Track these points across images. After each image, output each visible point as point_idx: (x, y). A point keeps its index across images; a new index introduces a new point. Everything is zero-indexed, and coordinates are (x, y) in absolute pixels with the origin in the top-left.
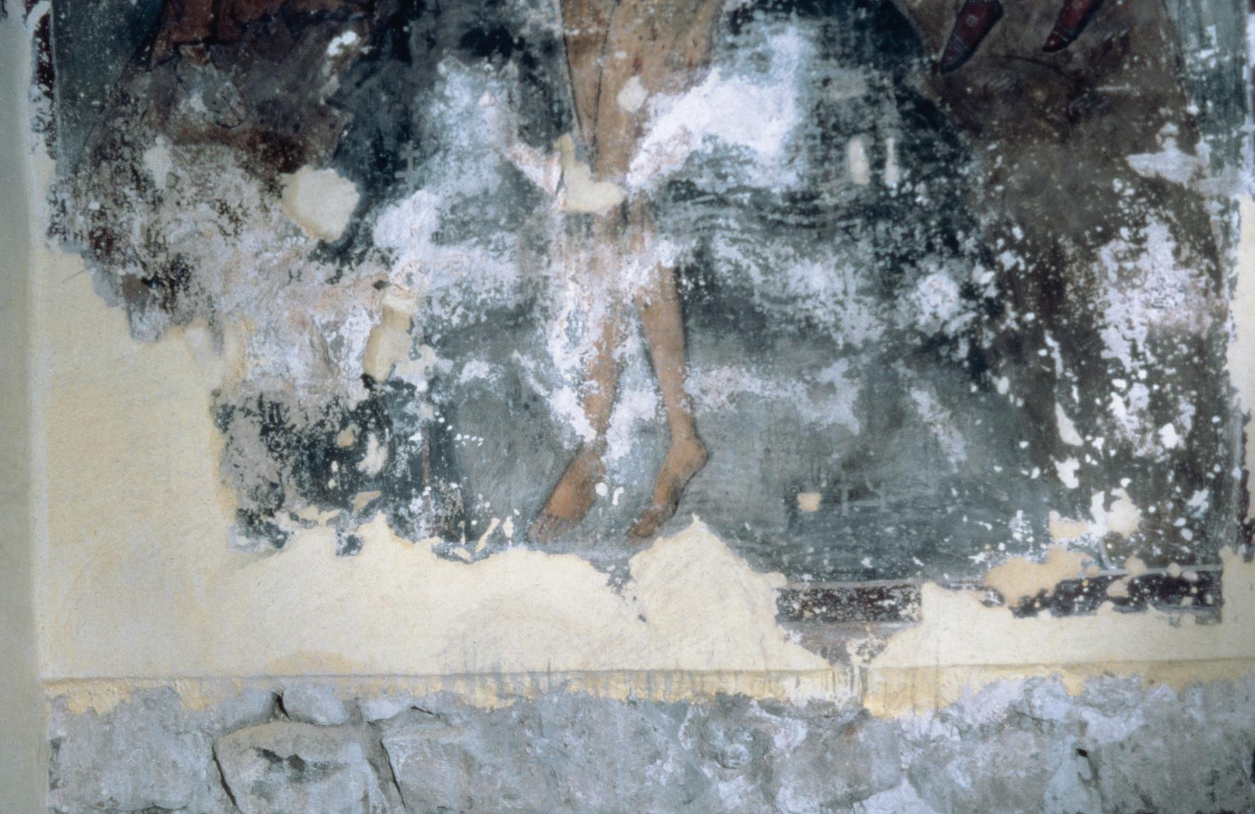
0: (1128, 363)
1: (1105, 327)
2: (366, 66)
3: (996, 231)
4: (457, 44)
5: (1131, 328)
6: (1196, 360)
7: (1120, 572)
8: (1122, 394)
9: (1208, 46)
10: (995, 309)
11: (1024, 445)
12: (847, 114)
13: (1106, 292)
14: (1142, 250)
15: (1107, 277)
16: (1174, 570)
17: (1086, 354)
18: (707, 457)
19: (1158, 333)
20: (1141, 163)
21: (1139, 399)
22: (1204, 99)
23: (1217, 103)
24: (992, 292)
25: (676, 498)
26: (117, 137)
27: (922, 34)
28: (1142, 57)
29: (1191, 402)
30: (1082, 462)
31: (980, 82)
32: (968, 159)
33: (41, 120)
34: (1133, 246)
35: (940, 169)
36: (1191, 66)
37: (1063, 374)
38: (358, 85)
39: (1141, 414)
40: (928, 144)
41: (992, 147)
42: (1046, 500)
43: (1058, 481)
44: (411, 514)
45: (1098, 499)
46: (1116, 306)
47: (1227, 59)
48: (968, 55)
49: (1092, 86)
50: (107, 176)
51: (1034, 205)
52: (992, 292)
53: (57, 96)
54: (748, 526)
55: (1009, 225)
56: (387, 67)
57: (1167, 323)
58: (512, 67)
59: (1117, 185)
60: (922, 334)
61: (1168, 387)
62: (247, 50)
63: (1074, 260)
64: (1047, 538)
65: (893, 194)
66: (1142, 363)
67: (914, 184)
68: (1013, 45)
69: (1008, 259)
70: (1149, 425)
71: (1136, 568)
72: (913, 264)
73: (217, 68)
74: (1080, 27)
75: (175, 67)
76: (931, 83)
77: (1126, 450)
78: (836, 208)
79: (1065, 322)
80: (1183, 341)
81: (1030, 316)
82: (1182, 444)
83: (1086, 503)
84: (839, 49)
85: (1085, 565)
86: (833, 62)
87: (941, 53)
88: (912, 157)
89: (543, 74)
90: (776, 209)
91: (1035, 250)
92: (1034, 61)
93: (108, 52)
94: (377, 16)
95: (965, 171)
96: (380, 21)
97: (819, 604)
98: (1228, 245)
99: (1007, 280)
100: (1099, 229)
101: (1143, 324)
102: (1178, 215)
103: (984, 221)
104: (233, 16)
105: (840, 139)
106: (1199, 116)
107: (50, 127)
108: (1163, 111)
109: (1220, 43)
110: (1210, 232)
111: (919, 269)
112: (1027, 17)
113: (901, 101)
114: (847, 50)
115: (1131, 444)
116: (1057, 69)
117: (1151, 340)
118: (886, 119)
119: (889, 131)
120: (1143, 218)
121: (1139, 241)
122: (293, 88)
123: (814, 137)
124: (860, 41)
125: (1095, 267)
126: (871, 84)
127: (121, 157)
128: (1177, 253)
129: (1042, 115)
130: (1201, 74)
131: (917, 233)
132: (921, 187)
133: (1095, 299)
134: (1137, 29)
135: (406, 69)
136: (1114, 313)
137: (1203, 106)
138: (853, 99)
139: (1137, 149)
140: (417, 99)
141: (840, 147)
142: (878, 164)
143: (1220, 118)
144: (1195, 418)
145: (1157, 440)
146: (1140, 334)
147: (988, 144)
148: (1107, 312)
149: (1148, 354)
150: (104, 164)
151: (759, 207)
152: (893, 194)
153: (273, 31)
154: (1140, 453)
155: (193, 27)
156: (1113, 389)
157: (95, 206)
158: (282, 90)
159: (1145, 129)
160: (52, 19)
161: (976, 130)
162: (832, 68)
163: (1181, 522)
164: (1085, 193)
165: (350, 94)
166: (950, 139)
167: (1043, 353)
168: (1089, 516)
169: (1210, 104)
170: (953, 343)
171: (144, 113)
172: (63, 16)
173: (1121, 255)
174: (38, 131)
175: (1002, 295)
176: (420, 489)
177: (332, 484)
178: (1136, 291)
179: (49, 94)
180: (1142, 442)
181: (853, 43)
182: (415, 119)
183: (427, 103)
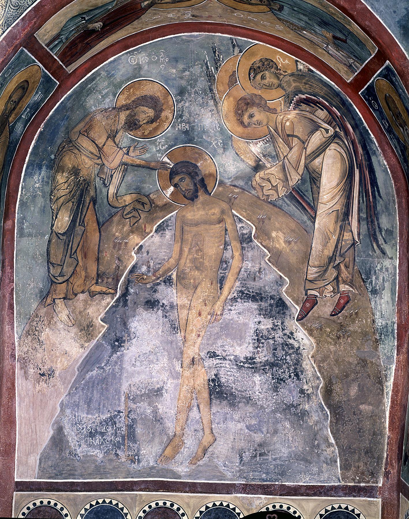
12: (265, 333)
72: (284, 381)
78: (261, 362)
84: (264, 312)
86: (262, 316)
105: (263, 341)
123: (255, 340)
124: (271, 310)
127: (35, 334)
129: (329, 336)
162: (261, 318)
181: (269, 310)
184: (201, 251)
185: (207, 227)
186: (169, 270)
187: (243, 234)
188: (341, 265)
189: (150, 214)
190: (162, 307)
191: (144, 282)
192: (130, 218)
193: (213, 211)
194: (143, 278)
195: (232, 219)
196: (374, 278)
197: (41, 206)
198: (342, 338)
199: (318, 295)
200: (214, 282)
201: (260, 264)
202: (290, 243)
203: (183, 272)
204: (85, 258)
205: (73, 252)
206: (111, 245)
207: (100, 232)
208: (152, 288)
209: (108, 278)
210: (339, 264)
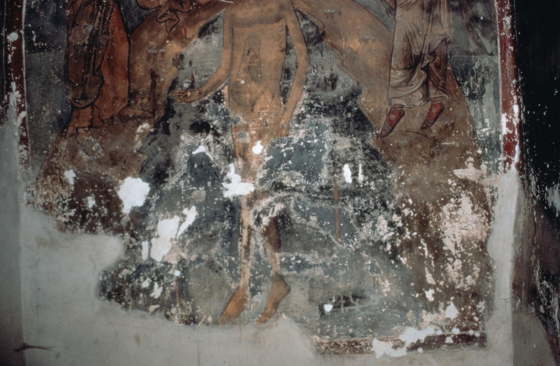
0: (454, 251)
1: (444, 237)
2: (152, 137)
3: (402, 201)
4: (189, 128)
5: (455, 238)
6: (480, 250)
7: (450, 333)
8: (451, 264)
9: (486, 127)
10: (401, 231)
11: (412, 284)
12: (343, 155)
13: (445, 224)
14: (459, 207)
15: (445, 218)
16: (471, 332)
17: (437, 249)
18: (289, 290)
19: (465, 239)
20: (459, 173)
21: (458, 266)
22: (484, 148)
23: (489, 149)
24: (400, 224)
25: (276, 305)
26: (54, 165)
27: (373, 123)
28: (459, 131)
29: (478, 267)
30: (435, 290)
31: (396, 142)
32: (391, 172)
33: (23, 159)
34: (456, 206)
35: (380, 176)
36: (479, 135)
37: (428, 256)
38: (149, 144)
39: (459, 271)
40: (375, 166)
41: (401, 167)
42: (421, 306)
43: (426, 299)
44: (172, 314)
45: (442, 304)
46: (449, 229)
47: (493, 132)
48: (391, 131)
49: (439, 143)
50: (50, 181)
51: (417, 190)
52: (400, 224)
53: (30, 149)
54: (304, 318)
55: (407, 198)
56: (161, 137)
57: (469, 236)
58: (210, 137)
59: (450, 182)
60: (373, 241)
61: (469, 260)
62: (105, 130)
63: (433, 211)
64: (422, 320)
65: (361, 186)
66: (459, 251)
67: (369, 182)
68: (409, 127)
69: (406, 212)
70: (462, 276)
71: (456, 331)
72: (369, 213)
73: (93, 137)
74: (435, 120)
75: (77, 138)
76: (376, 142)
77: (453, 285)
79: (429, 236)
80: (475, 243)
81: (415, 234)
82: (474, 283)
83: (437, 306)
84: (340, 129)
85: (436, 330)
86: (338, 134)
87: (380, 131)
88: (369, 171)
89: (223, 140)
90: (315, 193)
91: (417, 208)
92: (417, 133)
93: (50, 132)
94: (156, 117)
95: (390, 177)
96: (157, 119)
97: (332, 347)
98: (493, 204)
99: (405, 220)
100: (442, 199)
101: (459, 236)
102: (474, 193)
103: (397, 197)
104: (99, 117)
105: (340, 165)
106: (482, 154)
107: (27, 162)
108: (468, 152)
109: (490, 126)
110: (486, 200)
111: (371, 216)
112: (414, 115)
113: (364, 149)
114: (343, 130)
115: (455, 284)
116: (426, 136)
117: (462, 242)
118: (359, 156)
119: (359, 161)
120: (460, 195)
121: (458, 204)
122: (123, 146)
123: (330, 164)
124: (349, 127)
125: (441, 214)
126: (352, 143)
127: (55, 173)
128: (473, 208)
130: (483, 138)
131: (371, 202)
132: (372, 183)
133: (440, 226)
134: (458, 120)
135: (168, 138)
136: (448, 232)
137: (483, 150)
138: (345, 149)
139: (457, 168)
140: (173, 150)
141: (341, 168)
142: (355, 174)
143: (490, 154)
144: (480, 273)
145: (465, 282)
146: (458, 240)
147: (398, 166)
148: (445, 231)
149: (462, 248)
150: (49, 176)
151: (308, 192)
152: (361, 186)
153: (115, 123)
154: (458, 287)
155: (83, 122)
156: (448, 262)
157: (45, 193)
158: (119, 146)
159: (461, 160)
160: (27, 119)
161: (394, 160)
162: (337, 137)
163: (474, 314)
164: (436, 185)
165: (146, 148)
166: (383, 164)
167: (420, 248)
168: (438, 311)
169: (486, 149)
170: (385, 245)
171: (64, 156)
172: (31, 118)
173: (451, 209)
174: (22, 164)
175: (404, 225)
176: (175, 304)
177: (140, 302)
178: (457, 223)
179: (26, 149)
180: (459, 282)
182: (172, 157)
183: (176, 151)
184: (257, 57)
185: (263, 26)
186: (219, 82)
187: (309, 34)
188: (430, 65)
189: (191, 15)
190: (213, 129)
191: (189, 100)
192: (165, 21)
193: (269, 6)
194: (186, 96)
195: (294, 15)
196: (472, 78)
197: (53, 12)
198: (436, 156)
199: (405, 104)
200: (276, 96)
201: (332, 70)
202: (366, 41)
203: (237, 84)
204: (113, 74)
205: (96, 68)
206: (144, 57)
207: (129, 41)
208: (199, 107)
209: (142, 98)
210: (428, 64)
